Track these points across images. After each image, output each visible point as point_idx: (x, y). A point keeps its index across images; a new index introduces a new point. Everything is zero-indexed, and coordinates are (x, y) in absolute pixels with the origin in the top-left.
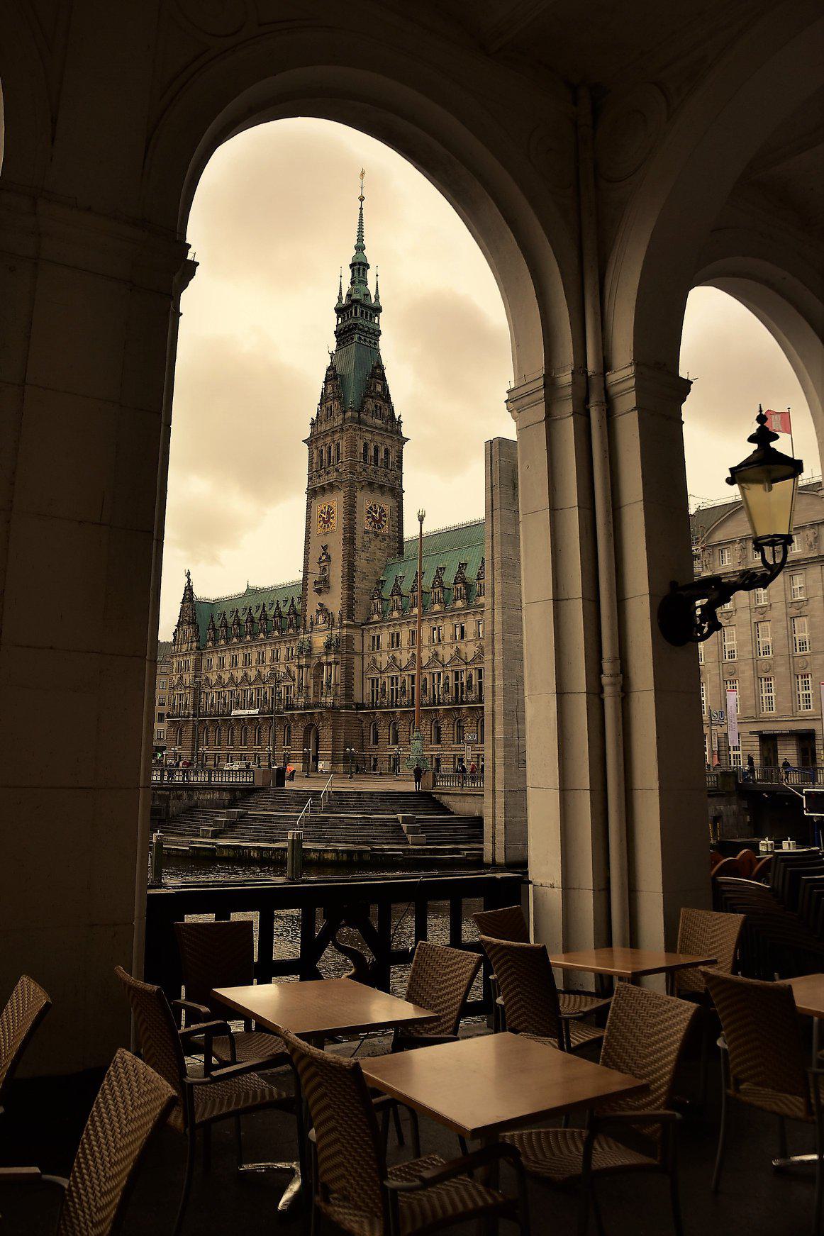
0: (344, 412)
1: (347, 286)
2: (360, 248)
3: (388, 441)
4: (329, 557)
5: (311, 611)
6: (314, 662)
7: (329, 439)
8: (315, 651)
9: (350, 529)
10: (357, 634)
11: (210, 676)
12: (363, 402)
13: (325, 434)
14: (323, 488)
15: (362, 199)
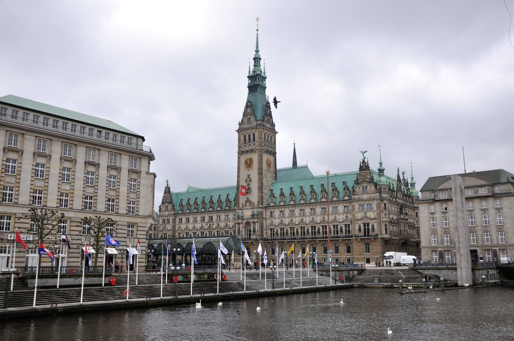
0: (257, 121)
1: (252, 68)
2: (257, 51)
3: (272, 133)
4: (251, 180)
5: (242, 200)
6: (244, 222)
7: (249, 131)
8: (245, 217)
9: (260, 169)
10: (264, 210)
11: (181, 226)
12: (264, 118)
13: (248, 129)
14: (247, 151)
15: (257, 30)
